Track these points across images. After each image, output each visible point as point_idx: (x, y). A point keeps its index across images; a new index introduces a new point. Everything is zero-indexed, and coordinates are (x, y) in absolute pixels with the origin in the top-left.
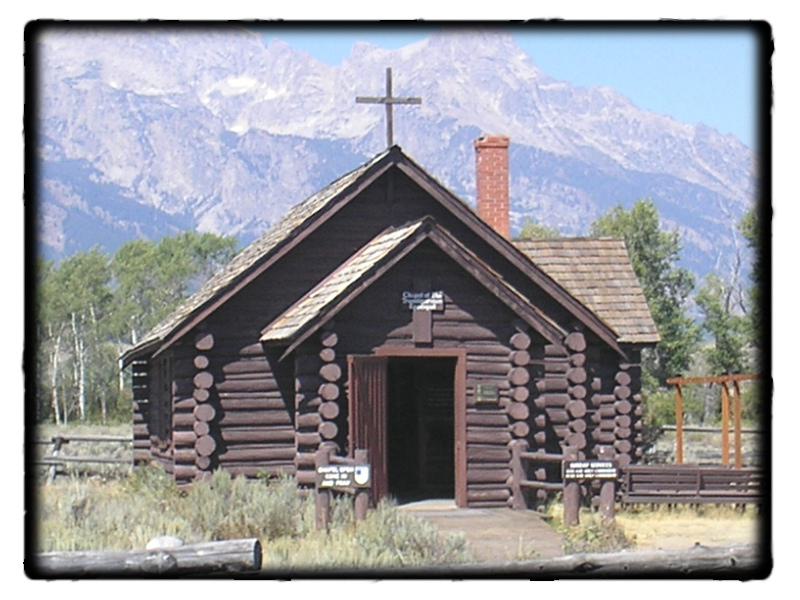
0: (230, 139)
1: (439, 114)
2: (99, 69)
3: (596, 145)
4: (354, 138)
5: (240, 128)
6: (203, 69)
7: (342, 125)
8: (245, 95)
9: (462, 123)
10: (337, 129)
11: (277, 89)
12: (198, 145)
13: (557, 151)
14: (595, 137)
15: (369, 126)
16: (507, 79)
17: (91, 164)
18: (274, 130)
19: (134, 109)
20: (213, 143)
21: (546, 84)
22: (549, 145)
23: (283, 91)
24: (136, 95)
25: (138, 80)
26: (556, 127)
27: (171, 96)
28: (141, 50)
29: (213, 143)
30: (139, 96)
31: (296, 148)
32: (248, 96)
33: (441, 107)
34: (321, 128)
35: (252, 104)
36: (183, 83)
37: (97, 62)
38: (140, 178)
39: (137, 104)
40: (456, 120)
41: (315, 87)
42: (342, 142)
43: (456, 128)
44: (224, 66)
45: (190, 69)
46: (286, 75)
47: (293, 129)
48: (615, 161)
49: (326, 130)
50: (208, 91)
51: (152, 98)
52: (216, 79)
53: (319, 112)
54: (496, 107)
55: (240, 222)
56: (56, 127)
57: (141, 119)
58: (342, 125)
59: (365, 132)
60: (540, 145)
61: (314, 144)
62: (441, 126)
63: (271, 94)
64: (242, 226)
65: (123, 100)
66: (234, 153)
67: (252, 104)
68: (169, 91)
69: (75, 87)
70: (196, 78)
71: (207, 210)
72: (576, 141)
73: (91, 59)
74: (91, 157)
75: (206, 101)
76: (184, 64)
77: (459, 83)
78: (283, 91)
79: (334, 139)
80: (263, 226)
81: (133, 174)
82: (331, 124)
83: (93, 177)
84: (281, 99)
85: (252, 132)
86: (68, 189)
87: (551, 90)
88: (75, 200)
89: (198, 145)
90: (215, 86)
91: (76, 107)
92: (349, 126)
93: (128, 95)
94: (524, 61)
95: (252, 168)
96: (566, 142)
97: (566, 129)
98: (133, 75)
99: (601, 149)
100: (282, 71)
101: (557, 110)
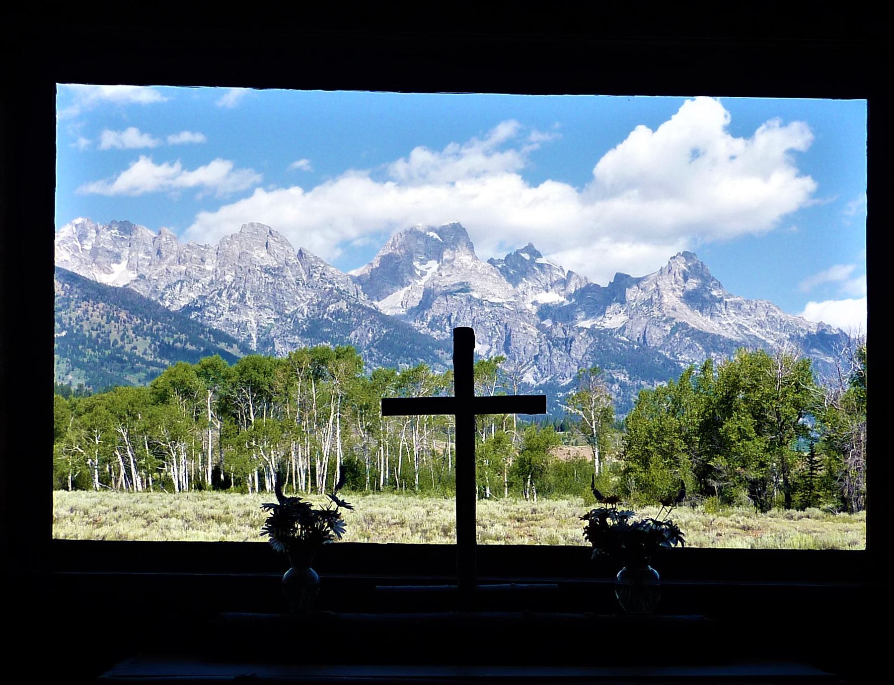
3: (757, 334)
4: (614, 328)
6: (528, 288)
9: (678, 320)
12: (524, 332)
13: (734, 338)
14: (757, 329)
20: (533, 331)
22: (730, 334)
25: (490, 294)
26: (734, 323)
27: (509, 303)
29: (533, 331)
30: (492, 303)
31: (581, 334)
36: (516, 296)
37: (467, 283)
40: (674, 318)
41: (592, 299)
42: (605, 331)
43: (674, 323)
44: (539, 286)
48: (769, 344)
50: (531, 301)
55: (547, 377)
59: (621, 325)
60: (724, 334)
62: (666, 322)
64: (548, 378)
68: (508, 300)
70: (524, 293)
71: (529, 369)
72: (745, 332)
75: (529, 306)
79: (603, 328)
84: (573, 304)
87: (731, 302)
89: (524, 332)
90: (535, 298)
92: (612, 321)
96: (739, 332)
97: (740, 324)
99: (760, 336)
101: (735, 313)
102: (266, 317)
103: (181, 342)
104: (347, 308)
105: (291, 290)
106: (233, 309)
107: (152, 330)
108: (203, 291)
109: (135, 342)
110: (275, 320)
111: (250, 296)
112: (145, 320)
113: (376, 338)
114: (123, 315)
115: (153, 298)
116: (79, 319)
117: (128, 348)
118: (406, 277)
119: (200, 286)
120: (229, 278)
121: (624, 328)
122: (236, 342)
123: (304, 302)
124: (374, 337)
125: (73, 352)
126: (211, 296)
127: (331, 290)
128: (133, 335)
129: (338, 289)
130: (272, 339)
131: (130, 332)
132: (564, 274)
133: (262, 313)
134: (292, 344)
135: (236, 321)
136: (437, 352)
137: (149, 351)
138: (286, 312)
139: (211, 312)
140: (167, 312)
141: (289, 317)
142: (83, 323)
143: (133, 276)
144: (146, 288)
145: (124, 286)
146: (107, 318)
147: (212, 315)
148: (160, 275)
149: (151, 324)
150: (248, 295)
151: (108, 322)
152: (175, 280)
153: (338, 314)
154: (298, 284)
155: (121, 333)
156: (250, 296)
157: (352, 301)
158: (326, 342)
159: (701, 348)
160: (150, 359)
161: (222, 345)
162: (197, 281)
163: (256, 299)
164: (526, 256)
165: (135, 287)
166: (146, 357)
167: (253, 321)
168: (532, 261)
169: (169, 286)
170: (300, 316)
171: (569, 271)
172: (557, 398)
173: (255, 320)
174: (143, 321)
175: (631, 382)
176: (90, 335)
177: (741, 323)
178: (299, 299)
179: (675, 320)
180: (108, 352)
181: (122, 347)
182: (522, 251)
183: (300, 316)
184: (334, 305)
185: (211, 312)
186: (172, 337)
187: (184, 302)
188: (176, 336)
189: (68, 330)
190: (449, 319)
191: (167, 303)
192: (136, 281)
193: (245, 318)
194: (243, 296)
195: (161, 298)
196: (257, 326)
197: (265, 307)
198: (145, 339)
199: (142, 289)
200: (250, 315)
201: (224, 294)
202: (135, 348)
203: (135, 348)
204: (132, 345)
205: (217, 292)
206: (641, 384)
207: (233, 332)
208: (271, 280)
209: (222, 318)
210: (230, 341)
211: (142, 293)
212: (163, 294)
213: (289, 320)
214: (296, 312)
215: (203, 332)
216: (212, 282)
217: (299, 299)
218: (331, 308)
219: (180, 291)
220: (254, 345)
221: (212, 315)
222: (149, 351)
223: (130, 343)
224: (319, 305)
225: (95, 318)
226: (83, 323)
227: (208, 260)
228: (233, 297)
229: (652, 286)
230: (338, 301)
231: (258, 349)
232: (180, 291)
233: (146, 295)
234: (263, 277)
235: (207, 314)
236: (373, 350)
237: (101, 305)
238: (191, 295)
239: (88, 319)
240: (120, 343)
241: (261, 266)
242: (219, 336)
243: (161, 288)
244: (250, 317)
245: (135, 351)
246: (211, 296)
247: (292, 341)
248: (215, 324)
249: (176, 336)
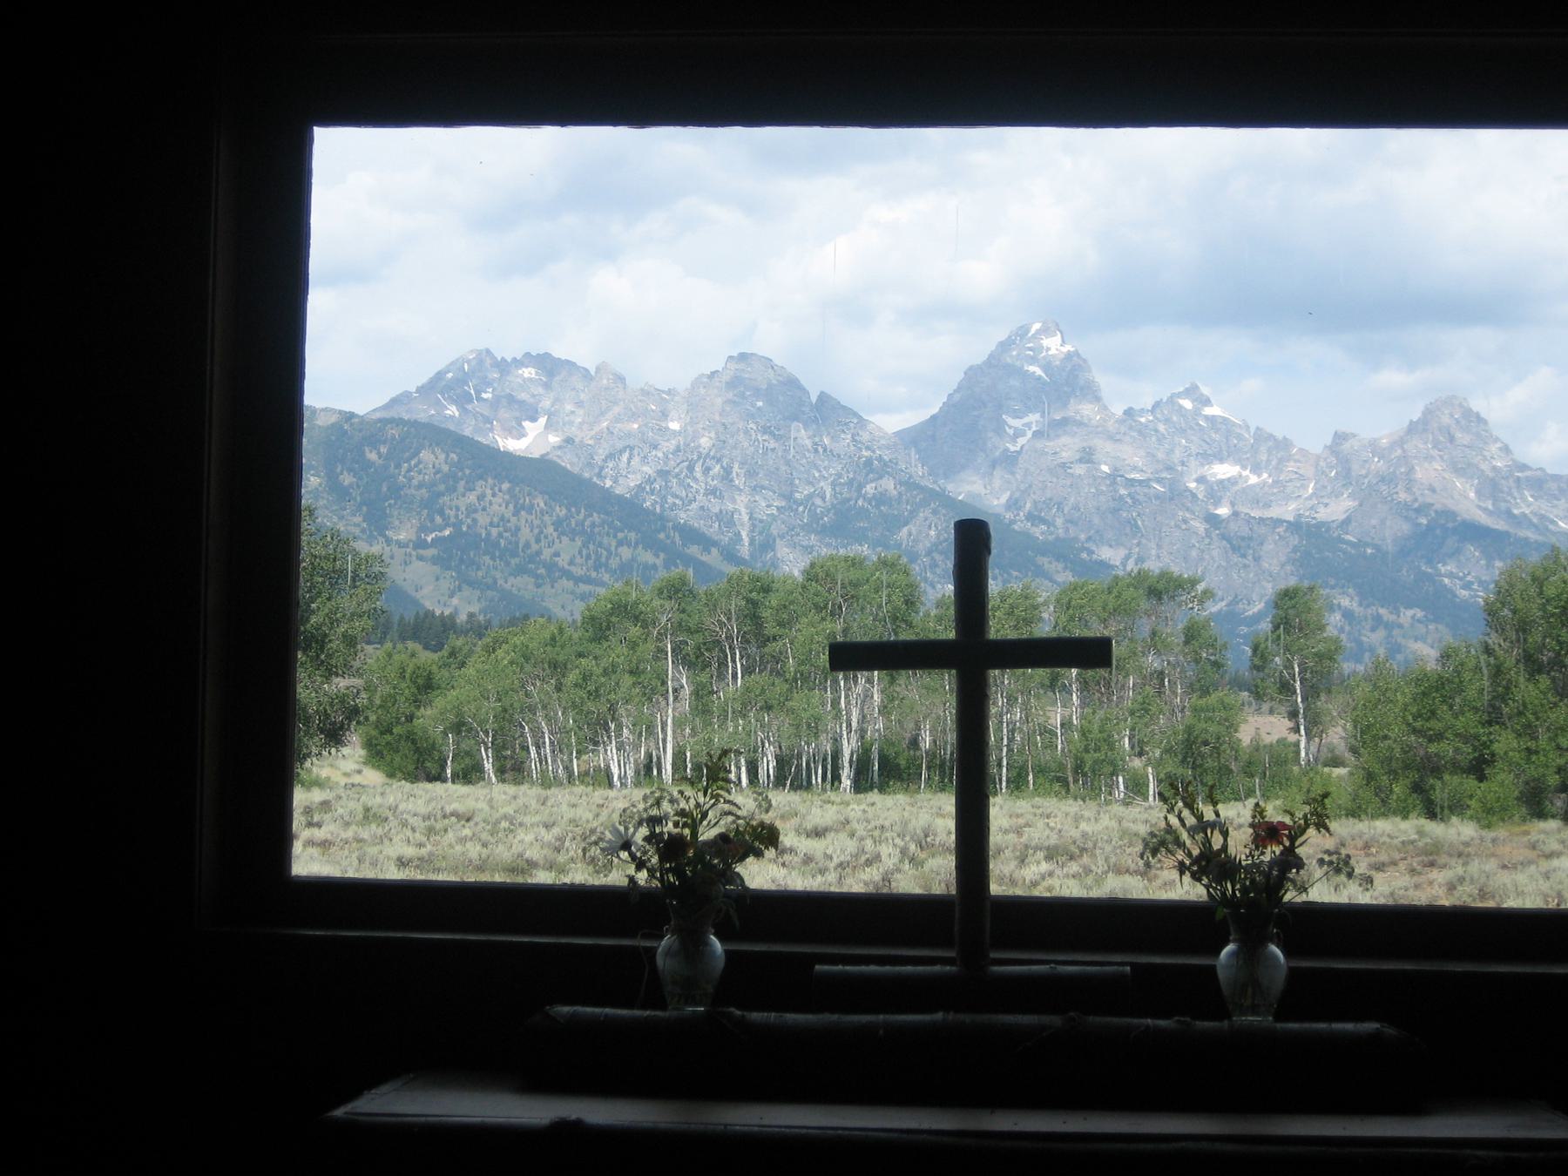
0: (1212, 520)
1: (1416, 500)
2: (1093, 455)
4: (1333, 521)
5: (1223, 511)
6: (1189, 455)
7: (1322, 509)
8: (1229, 479)
9: (1438, 507)
10: (1317, 512)
11: (1259, 476)
12: (1184, 527)
15: (1347, 511)
16: (1484, 466)
17: (1083, 543)
18: (1256, 513)
19: (1123, 492)
20: (1198, 525)
21: (1522, 471)
23: (1265, 475)
24: (1127, 479)
26: (1531, 512)
28: (1131, 437)
31: (1277, 530)
32: (1232, 481)
33: (1418, 493)
34: (1301, 512)
35: (1237, 488)
37: (1090, 448)
38: (1127, 558)
39: (1125, 487)
40: (1433, 505)
41: (1296, 473)
44: (1209, 452)
45: (1178, 455)
46: (1268, 461)
47: (1274, 512)
49: (1307, 514)
50: (1194, 476)
51: (1141, 482)
52: (1202, 465)
53: (1299, 496)
54: (1472, 495)
55: (1222, 600)
56: (1051, 509)
57: (1130, 501)
58: (1322, 509)
59: (1343, 517)
61: (1295, 526)
63: (1253, 479)
64: (1224, 603)
65: (1114, 483)
66: (1218, 535)
67: (1237, 488)
68: (1157, 476)
69: (1069, 471)
73: (1085, 444)
74: (1083, 537)
75: (1193, 485)
76: (1172, 450)
77: (1436, 470)
78: (1265, 475)
79: (1314, 522)
80: (1243, 604)
81: (1122, 552)
82: (1311, 508)
83: (1084, 555)
84: (1264, 483)
85: (1236, 514)
86: (1060, 566)
87: (1527, 477)
88: (1067, 576)
89: (1184, 527)
91: (1070, 490)
92: (1329, 510)
93: (1119, 478)
94: (1500, 449)
95: (1235, 549)
97: (1542, 515)
98: (1125, 459)
100: (1264, 458)
101: (1532, 496)
102: (764, 505)
103: (629, 545)
104: (895, 488)
105: (804, 461)
106: (712, 492)
107: (583, 525)
108: (665, 463)
109: (557, 546)
110: (778, 508)
111: (739, 471)
112: (573, 510)
113: (942, 538)
114: (540, 502)
115: (586, 475)
116: (471, 510)
117: (547, 554)
118: (991, 438)
119: (660, 455)
120: (705, 442)
121: (1347, 522)
122: (715, 544)
124: (938, 536)
125: (462, 560)
126: (677, 470)
128: (555, 534)
129: (880, 458)
130: (774, 540)
131: (551, 529)
132: (1249, 433)
133: (757, 498)
134: (806, 548)
136: (1042, 560)
137: (578, 560)
138: (797, 495)
139: (677, 497)
140: (607, 495)
142: (478, 516)
143: (554, 439)
144: (575, 460)
145: (542, 456)
146: (515, 507)
147: (677, 501)
148: (598, 438)
149: (581, 516)
151: (516, 513)
152: (620, 445)
153: (881, 499)
154: (816, 451)
155: (536, 531)
156: (739, 471)
158: (861, 545)
159: (1477, 554)
160: (578, 571)
161: (694, 550)
162: (655, 447)
163: (751, 474)
164: (1187, 404)
165: (559, 457)
166: (573, 569)
167: (743, 510)
168: (1197, 413)
169: (610, 456)
170: (818, 502)
171: (1258, 428)
172: (1239, 636)
173: (747, 509)
174: (570, 511)
175: (1362, 609)
176: (489, 534)
177: (1543, 512)
178: (817, 475)
179: (1434, 508)
180: (514, 561)
181: (539, 553)
182: (1179, 395)
183: (818, 502)
185: (677, 497)
186: (615, 536)
187: (634, 481)
188: (620, 535)
189: (454, 525)
190: (1060, 506)
191: (608, 483)
192: (560, 447)
193: (730, 507)
194: (727, 471)
195: (599, 475)
196: (750, 519)
197: (763, 487)
198: (574, 540)
199: (569, 461)
200: (739, 501)
201: (698, 468)
202: (557, 554)
203: (557, 554)
204: (552, 550)
205: (686, 464)
206: (1378, 613)
207: (713, 530)
208: (772, 444)
209: (694, 506)
210: (707, 543)
211: (568, 466)
212: (602, 468)
214: (810, 496)
215: (663, 528)
216: (678, 449)
218: (869, 489)
219: (629, 462)
220: (745, 550)
221: (677, 501)
222: (578, 560)
223: (549, 547)
224: (850, 483)
225: (495, 507)
226: (478, 516)
227: (673, 414)
228: (711, 473)
229: (1396, 451)
230: (881, 478)
231: (752, 555)
232: (629, 462)
233: (576, 470)
234: (760, 440)
235: (670, 500)
236: (937, 556)
237: (505, 486)
238: (646, 469)
239: (484, 509)
240: (535, 547)
242: (691, 535)
243: (598, 459)
244: (740, 505)
245: (557, 559)
246: (677, 470)
247: (805, 543)
248: (683, 515)
249: (620, 535)
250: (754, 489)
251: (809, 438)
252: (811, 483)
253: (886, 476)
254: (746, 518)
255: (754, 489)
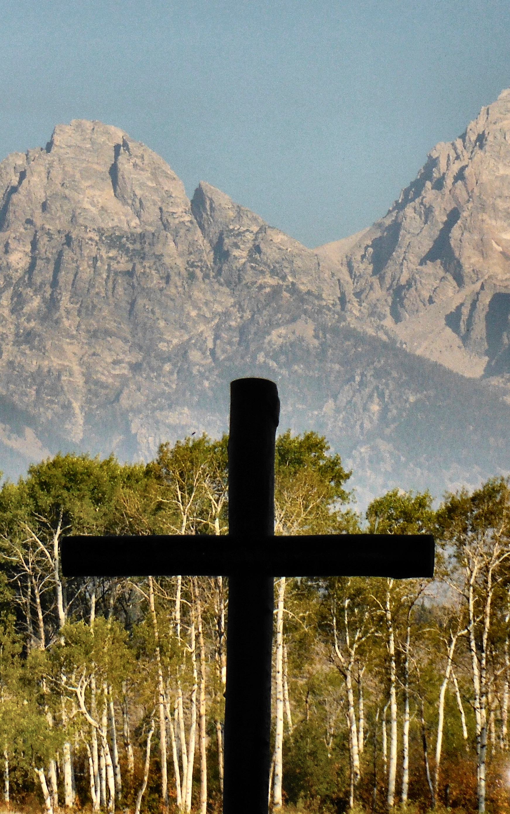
102: (109, 360)
104: (316, 337)
105: (173, 290)
111: (70, 306)
118: (469, 258)
123: (207, 321)
127: (276, 291)
129: (293, 289)
133: (98, 350)
135: (33, 365)
138: (162, 346)
141: (169, 359)
150: (65, 301)
154: (192, 276)
156: (70, 306)
157: (329, 319)
167: (76, 368)
173: (81, 365)
184: (282, 331)
193: (56, 362)
196: (86, 382)
197: (108, 333)
200: (70, 354)
213: (167, 367)
217: (193, 313)
228: (26, 309)
230: (293, 320)
234: (105, 256)
241: (100, 231)
250: (94, 335)
251: (181, 255)
252: (183, 327)
253: (303, 316)
254: (79, 380)
255: (94, 335)
